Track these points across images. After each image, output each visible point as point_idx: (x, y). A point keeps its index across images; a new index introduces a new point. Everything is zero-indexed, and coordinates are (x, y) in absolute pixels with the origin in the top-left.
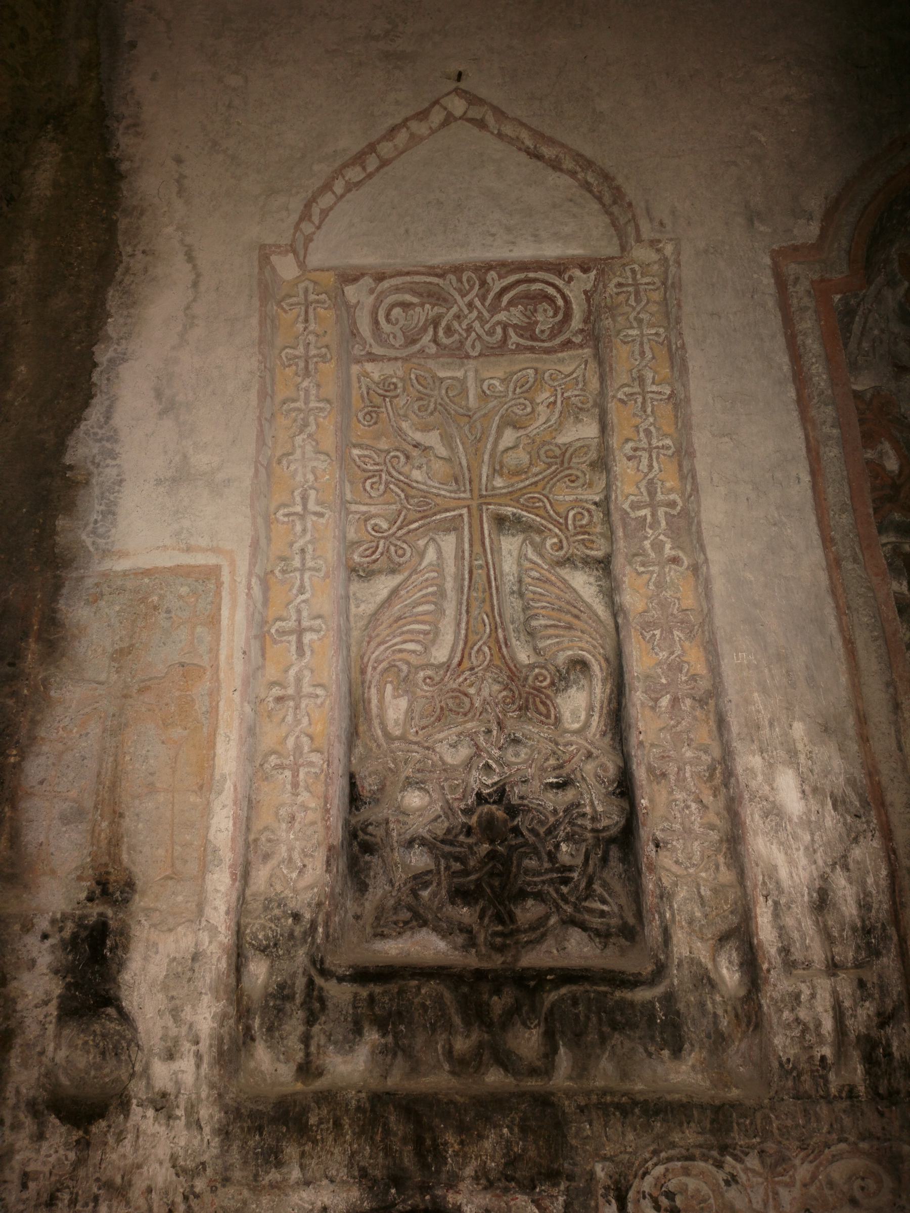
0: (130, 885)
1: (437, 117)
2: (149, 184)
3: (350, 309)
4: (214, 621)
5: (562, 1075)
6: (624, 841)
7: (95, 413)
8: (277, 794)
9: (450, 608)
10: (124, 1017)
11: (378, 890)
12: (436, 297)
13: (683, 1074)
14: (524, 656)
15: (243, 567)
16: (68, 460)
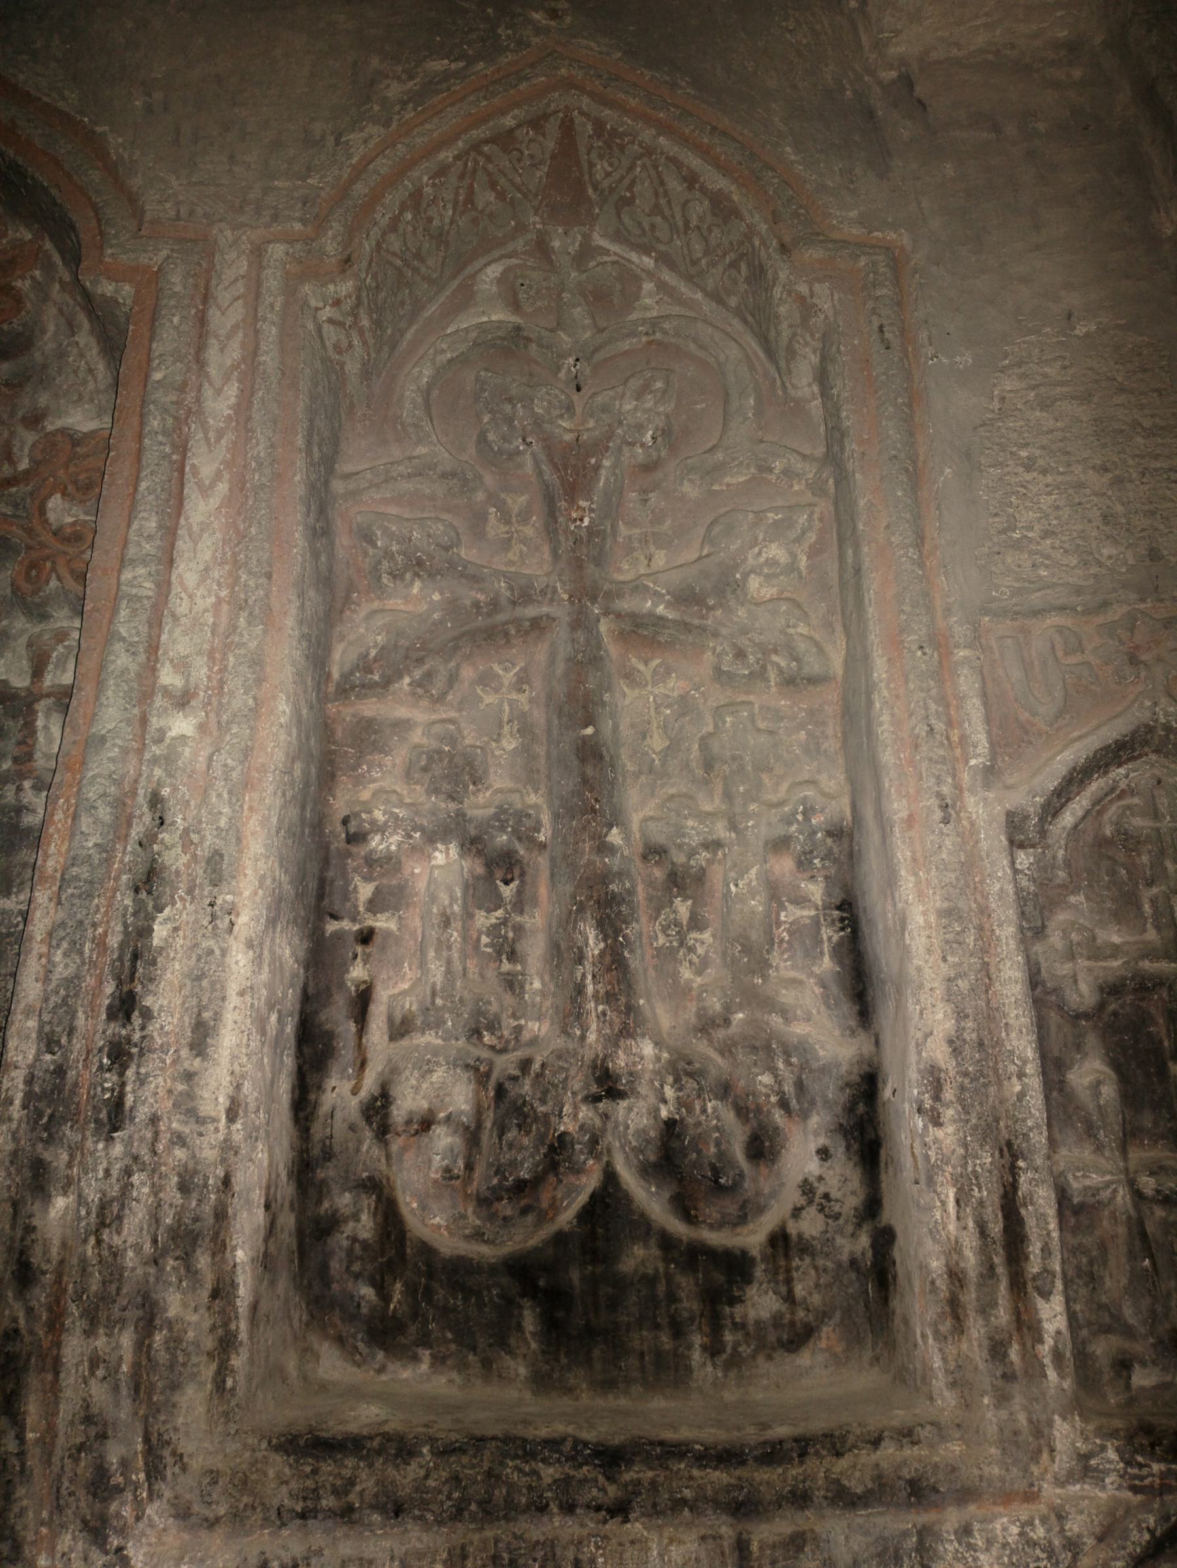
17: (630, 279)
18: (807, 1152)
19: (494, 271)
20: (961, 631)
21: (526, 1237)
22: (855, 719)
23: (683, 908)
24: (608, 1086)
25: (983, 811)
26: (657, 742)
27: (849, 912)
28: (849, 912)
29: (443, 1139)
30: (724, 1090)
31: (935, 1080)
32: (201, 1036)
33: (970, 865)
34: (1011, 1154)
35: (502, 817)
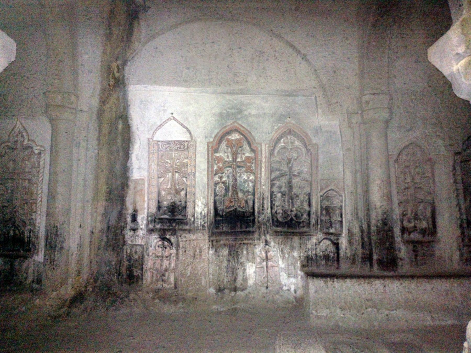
0: (137, 211)
2: (134, 128)
3: (159, 145)
4: (144, 185)
5: (177, 228)
6: (185, 207)
7: (130, 160)
8: (151, 202)
9: (170, 182)
10: (137, 222)
11: (161, 211)
12: (169, 144)
13: (187, 227)
14: (178, 187)
18: (305, 216)
19: (282, 140)
20: (319, 181)
21: (286, 221)
22: (311, 185)
24: (292, 211)
25: (319, 195)
26: (296, 184)
27: (309, 200)
29: (280, 214)
32: (268, 209)
33: (317, 199)
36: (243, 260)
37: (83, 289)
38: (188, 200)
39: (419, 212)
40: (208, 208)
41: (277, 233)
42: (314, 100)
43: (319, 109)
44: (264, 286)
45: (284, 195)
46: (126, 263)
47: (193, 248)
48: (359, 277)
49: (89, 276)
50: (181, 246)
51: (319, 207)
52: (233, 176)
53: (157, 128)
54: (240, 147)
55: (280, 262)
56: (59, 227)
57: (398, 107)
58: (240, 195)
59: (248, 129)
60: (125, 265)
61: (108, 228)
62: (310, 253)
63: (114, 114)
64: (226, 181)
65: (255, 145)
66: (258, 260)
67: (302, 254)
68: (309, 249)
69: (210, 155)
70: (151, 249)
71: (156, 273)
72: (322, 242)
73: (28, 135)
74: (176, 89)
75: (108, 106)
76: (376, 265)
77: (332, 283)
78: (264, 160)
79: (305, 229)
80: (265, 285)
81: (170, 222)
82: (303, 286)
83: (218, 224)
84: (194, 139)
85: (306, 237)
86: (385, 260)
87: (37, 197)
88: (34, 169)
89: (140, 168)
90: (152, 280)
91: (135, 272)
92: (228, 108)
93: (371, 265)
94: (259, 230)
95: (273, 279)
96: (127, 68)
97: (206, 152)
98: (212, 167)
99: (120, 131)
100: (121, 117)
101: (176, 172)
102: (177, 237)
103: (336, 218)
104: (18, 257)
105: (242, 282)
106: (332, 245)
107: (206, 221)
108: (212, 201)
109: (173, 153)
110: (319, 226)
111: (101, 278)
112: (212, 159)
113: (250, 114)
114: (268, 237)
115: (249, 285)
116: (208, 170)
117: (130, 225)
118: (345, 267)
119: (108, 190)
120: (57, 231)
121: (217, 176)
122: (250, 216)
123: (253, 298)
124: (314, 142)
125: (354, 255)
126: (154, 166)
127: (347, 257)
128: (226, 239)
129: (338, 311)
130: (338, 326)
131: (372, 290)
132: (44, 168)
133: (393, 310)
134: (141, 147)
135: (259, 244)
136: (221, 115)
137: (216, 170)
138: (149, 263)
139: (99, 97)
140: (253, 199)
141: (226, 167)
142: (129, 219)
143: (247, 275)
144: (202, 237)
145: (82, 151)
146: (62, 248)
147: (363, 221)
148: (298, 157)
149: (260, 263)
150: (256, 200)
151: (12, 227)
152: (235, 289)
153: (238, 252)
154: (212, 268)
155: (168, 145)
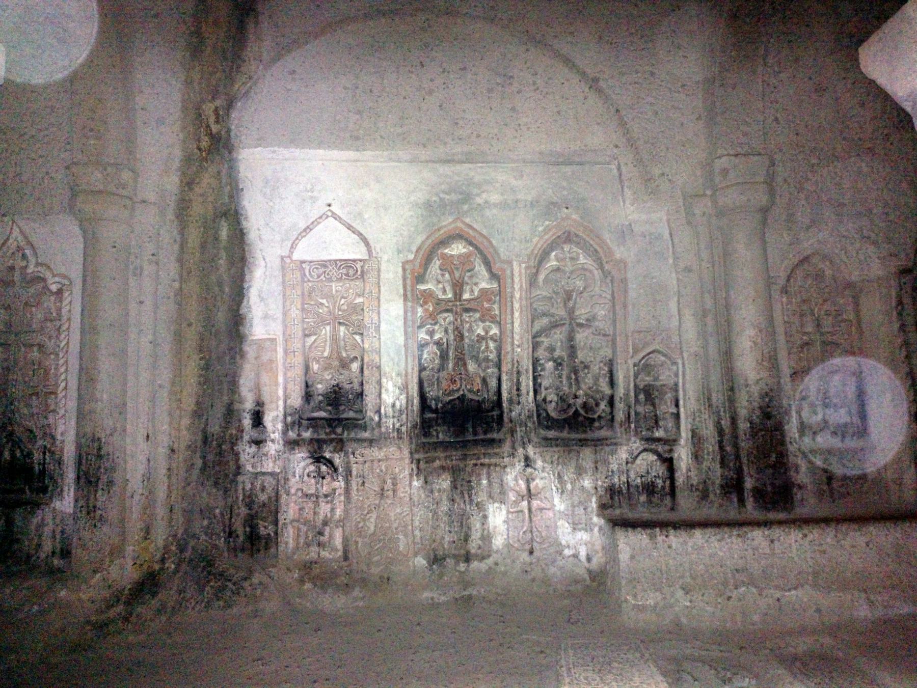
1: (324, 217)
3: (304, 269)
4: (276, 350)
6: (361, 395)
8: (290, 386)
9: (328, 344)
10: (264, 427)
11: (312, 404)
12: (325, 266)
13: (366, 435)
14: (344, 355)
15: (281, 338)
16: (241, 312)
17: (578, 254)
18: (603, 405)
19: (554, 253)
22: (614, 342)
23: (586, 371)
24: (576, 397)
25: (631, 362)
27: (611, 372)
28: (611, 372)
29: (553, 404)
30: (592, 397)
31: (621, 399)
32: (528, 393)
33: (628, 370)
34: (629, 407)
35: (559, 357)
36: (482, 497)
37: (157, 567)
38: (365, 379)
39: (832, 391)
40: (408, 393)
41: (547, 442)
42: (615, 171)
43: (626, 190)
44: (525, 550)
45: (560, 364)
46: (244, 511)
47: (379, 476)
48: (717, 524)
49: (167, 538)
50: (354, 473)
51: (632, 385)
52: (457, 328)
53: (300, 234)
54: (469, 271)
55: (557, 501)
56: (103, 440)
57: (785, 180)
58: (472, 367)
59: (484, 232)
60: (242, 515)
61: (205, 441)
62: (616, 480)
63: (210, 207)
64: (441, 339)
65: (498, 265)
66: (512, 496)
67: (600, 483)
68: (613, 472)
69: (409, 288)
70: (294, 483)
71: (304, 528)
72: (640, 458)
73: (36, 254)
74: (335, 153)
75: (198, 190)
76: (751, 499)
77: (664, 537)
78: (517, 295)
79: (604, 433)
80: (528, 547)
81: (330, 426)
82: (603, 548)
83: (430, 427)
84: (374, 255)
85: (607, 449)
86: (769, 489)
87: (57, 383)
88: (49, 324)
89: (266, 316)
90: (298, 543)
91: (262, 529)
92: (444, 192)
93: (742, 501)
94: (512, 435)
95: (543, 534)
96: (234, 114)
97: (401, 282)
98: (414, 312)
99: (224, 244)
100: (225, 214)
101: (340, 323)
102: (346, 454)
103: (665, 408)
104: (20, 504)
105: (480, 542)
106: (658, 463)
107: (405, 420)
108: (416, 380)
109: (333, 285)
110: (633, 426)
111: (192, 543)
112: (413, 295)
113: (486, 202)
114: (531, 451)
115: (495, 548)
116: (405, 319)
117: (249, 431)
118: (687, 505)
119: (203, 362)
120: (100, 449)
121: (424, 329)
122: (492, 409)
123: (505, 574)
124: (618, 256)
125: (705, 482)
126: (295, 312)
127: (692, 485)
128: (446, 457)
129: (680, 593)
130: (678, 624)
131: (746, 550)
132: (69, 320)
133: (789, 590)
134: (267, 273)
135: (513, 465)
136: (428, 205)
137: (422, 317)
138: (290, 510)
139: (179, 173)
140: (496, 375)
141: (441, 312)
142: (247, 422)
143: (491, 528)
144: (398, 454)
145: (148, 284)
146: (111, 483)
147: (722, 413)
148: (584, 288)
149: (516, 503)
150: (504, 377)
151: (7, 442)
152: (468, 558)
153: (469, 482)
154: (420, 516)
155: (323, 270)
